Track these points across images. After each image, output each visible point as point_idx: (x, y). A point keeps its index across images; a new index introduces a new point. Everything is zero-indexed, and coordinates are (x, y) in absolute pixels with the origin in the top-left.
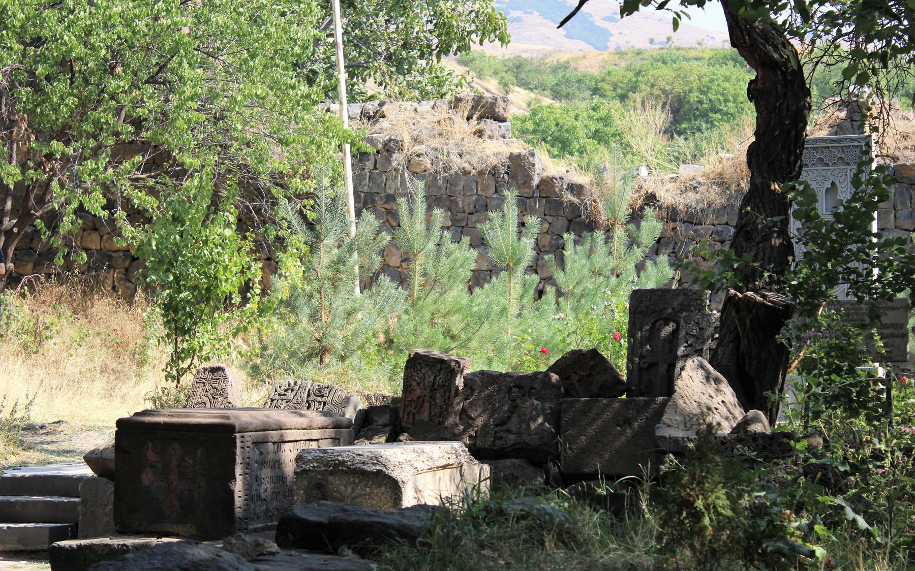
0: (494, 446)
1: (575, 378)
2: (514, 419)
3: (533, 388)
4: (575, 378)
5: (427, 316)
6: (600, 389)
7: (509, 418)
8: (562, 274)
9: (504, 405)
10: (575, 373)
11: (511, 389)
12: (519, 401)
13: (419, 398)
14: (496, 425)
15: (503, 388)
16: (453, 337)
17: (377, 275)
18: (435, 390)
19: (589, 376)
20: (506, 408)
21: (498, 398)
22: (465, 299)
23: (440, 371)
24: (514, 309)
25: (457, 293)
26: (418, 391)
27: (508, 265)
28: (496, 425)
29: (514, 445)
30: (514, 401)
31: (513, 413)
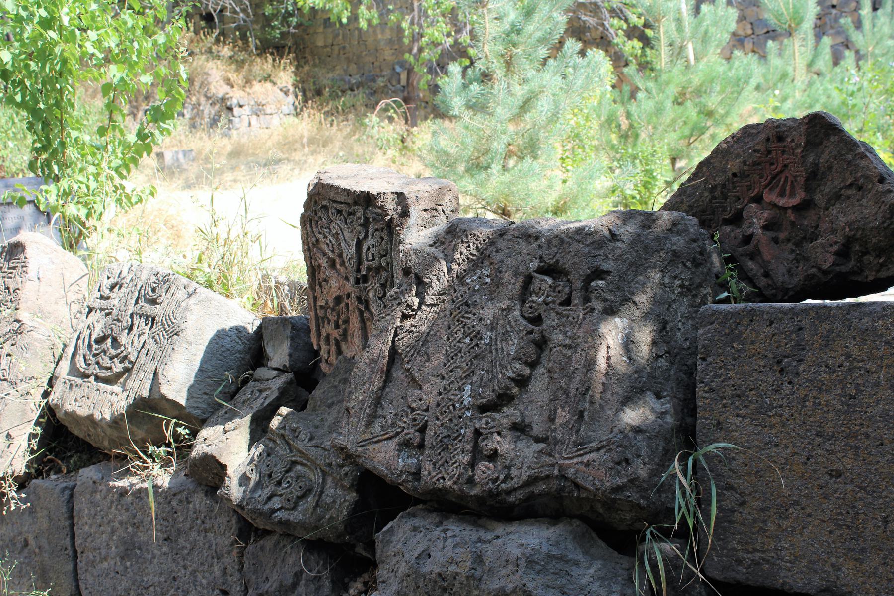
0: (471, 481)
1: (756, 220)
2: (539, 387)
3: (599, 273)
4: (756, 220)
5: (673, 90)
6: (844, 253)
7: (522, 382)
8: (861, 37)
9: (505, 336)
10: (758, 199)
11: (529, 279)
12: (551, 320)
13: (338, 300)
14: (483, 409)
15: (507, 276)
16: (710, 114)
17: (561, 43)
18: (365, 279)
19: (800, 208)
20: (512, 347)
21: (490, 312)
22: (721, 67)
23: (365, 225)
24: (801, 77)
25: (713, 60)
26: (334, 283)
27: (790, 26)
28: (483, 409)
29: (533, 480)
30: (537, 320)
31: (533, 365)
